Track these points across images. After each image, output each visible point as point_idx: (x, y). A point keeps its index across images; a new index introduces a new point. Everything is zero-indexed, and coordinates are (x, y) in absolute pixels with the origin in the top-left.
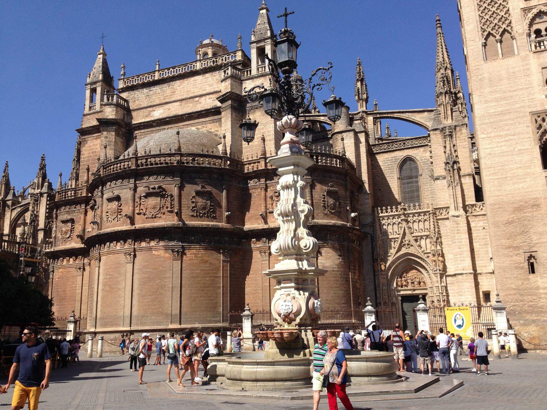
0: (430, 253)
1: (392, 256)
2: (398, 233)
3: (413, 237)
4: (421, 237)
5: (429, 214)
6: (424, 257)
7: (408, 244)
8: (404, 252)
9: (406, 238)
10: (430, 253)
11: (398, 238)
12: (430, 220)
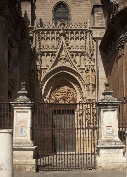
0: (84, 69)
1: (49, 69)
2: (55, 47)
3: (71, 52)
4: (77, 53)
5: (86, 33)
6: (79, 71)
7: (65, 59)
8: (60, 66)
9: (63, 53)
10: (84, 69)
11: (55, 52)
12: (86, 38)
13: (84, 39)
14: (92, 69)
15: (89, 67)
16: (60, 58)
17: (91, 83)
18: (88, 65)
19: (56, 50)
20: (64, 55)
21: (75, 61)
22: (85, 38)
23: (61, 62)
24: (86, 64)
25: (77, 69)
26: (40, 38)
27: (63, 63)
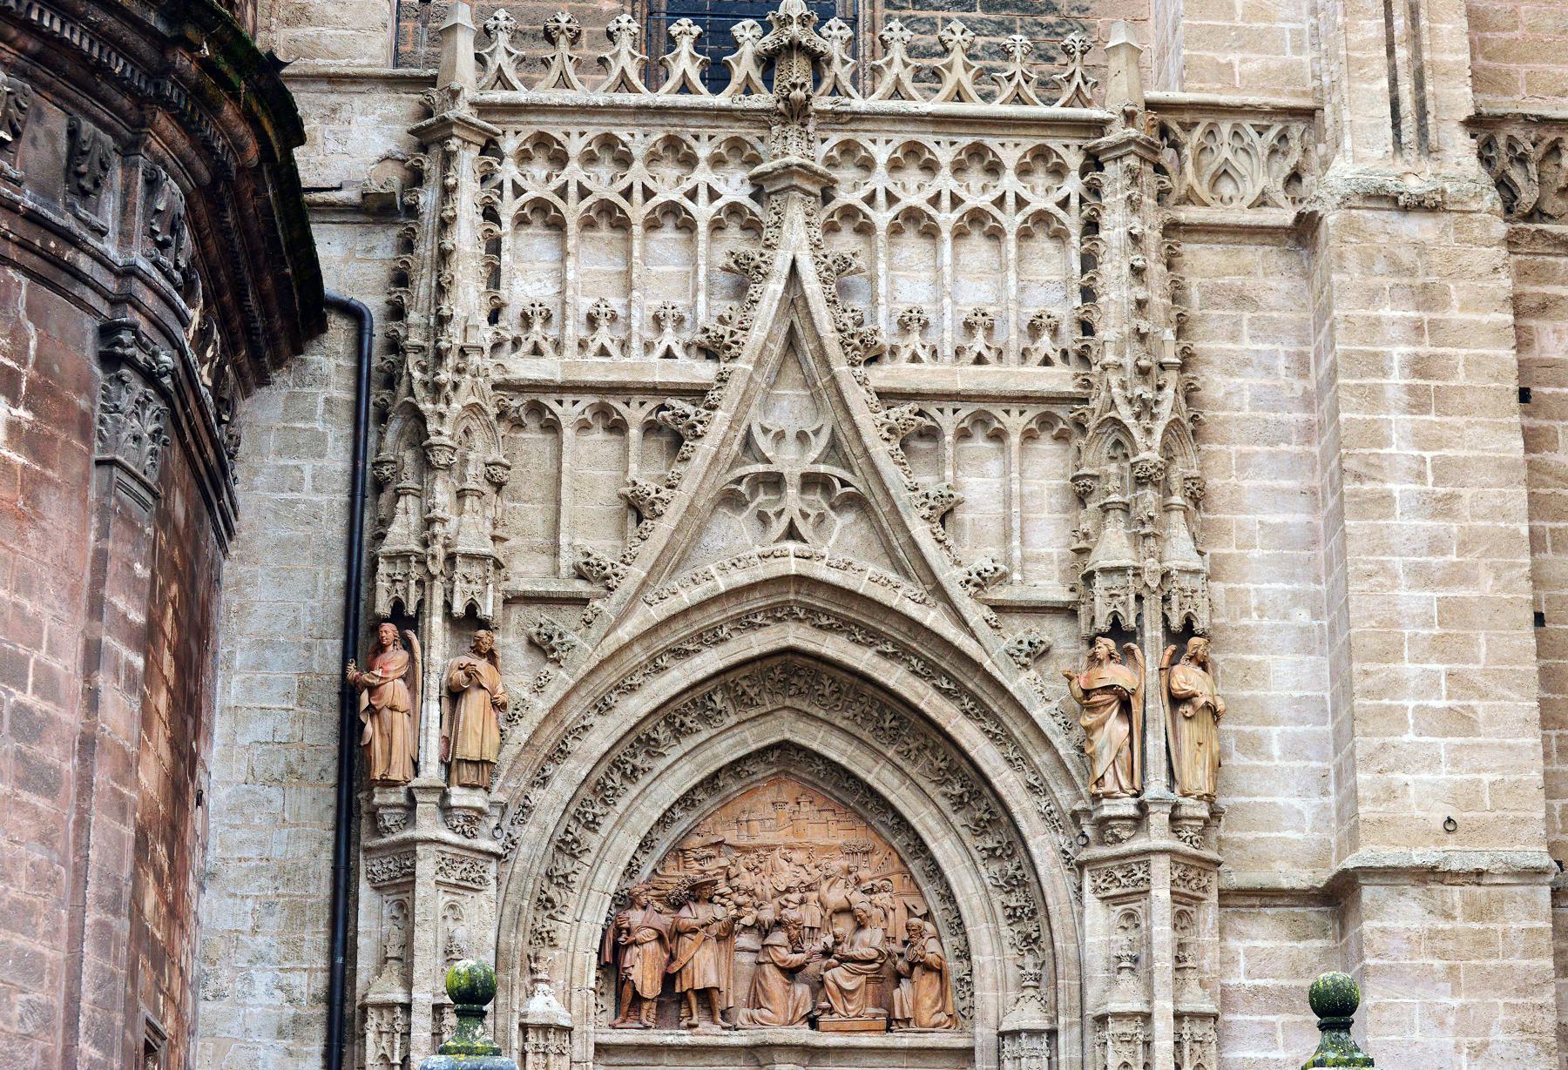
3: (887, 397)
7: (810, 482)
12: (1091, 227)
13: (1060, 236)
14: (1176, 622)
15: (1139, 598)
16: (761, 468)
17: (1159, 801)
18: (1121, 570)
19: (704, 371)
20: (802, 437)
21: (945, 514)
22: (1073, 221)
23: (763, 518)
24: (1099, 560)
25: (976, 614)
26: (508, 208)
27: (792, 533)
